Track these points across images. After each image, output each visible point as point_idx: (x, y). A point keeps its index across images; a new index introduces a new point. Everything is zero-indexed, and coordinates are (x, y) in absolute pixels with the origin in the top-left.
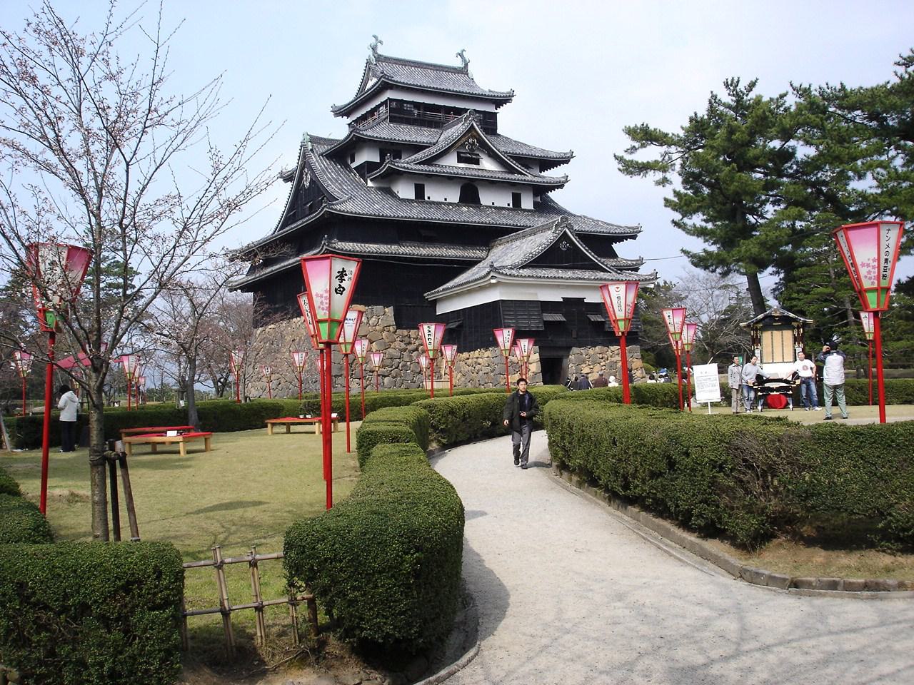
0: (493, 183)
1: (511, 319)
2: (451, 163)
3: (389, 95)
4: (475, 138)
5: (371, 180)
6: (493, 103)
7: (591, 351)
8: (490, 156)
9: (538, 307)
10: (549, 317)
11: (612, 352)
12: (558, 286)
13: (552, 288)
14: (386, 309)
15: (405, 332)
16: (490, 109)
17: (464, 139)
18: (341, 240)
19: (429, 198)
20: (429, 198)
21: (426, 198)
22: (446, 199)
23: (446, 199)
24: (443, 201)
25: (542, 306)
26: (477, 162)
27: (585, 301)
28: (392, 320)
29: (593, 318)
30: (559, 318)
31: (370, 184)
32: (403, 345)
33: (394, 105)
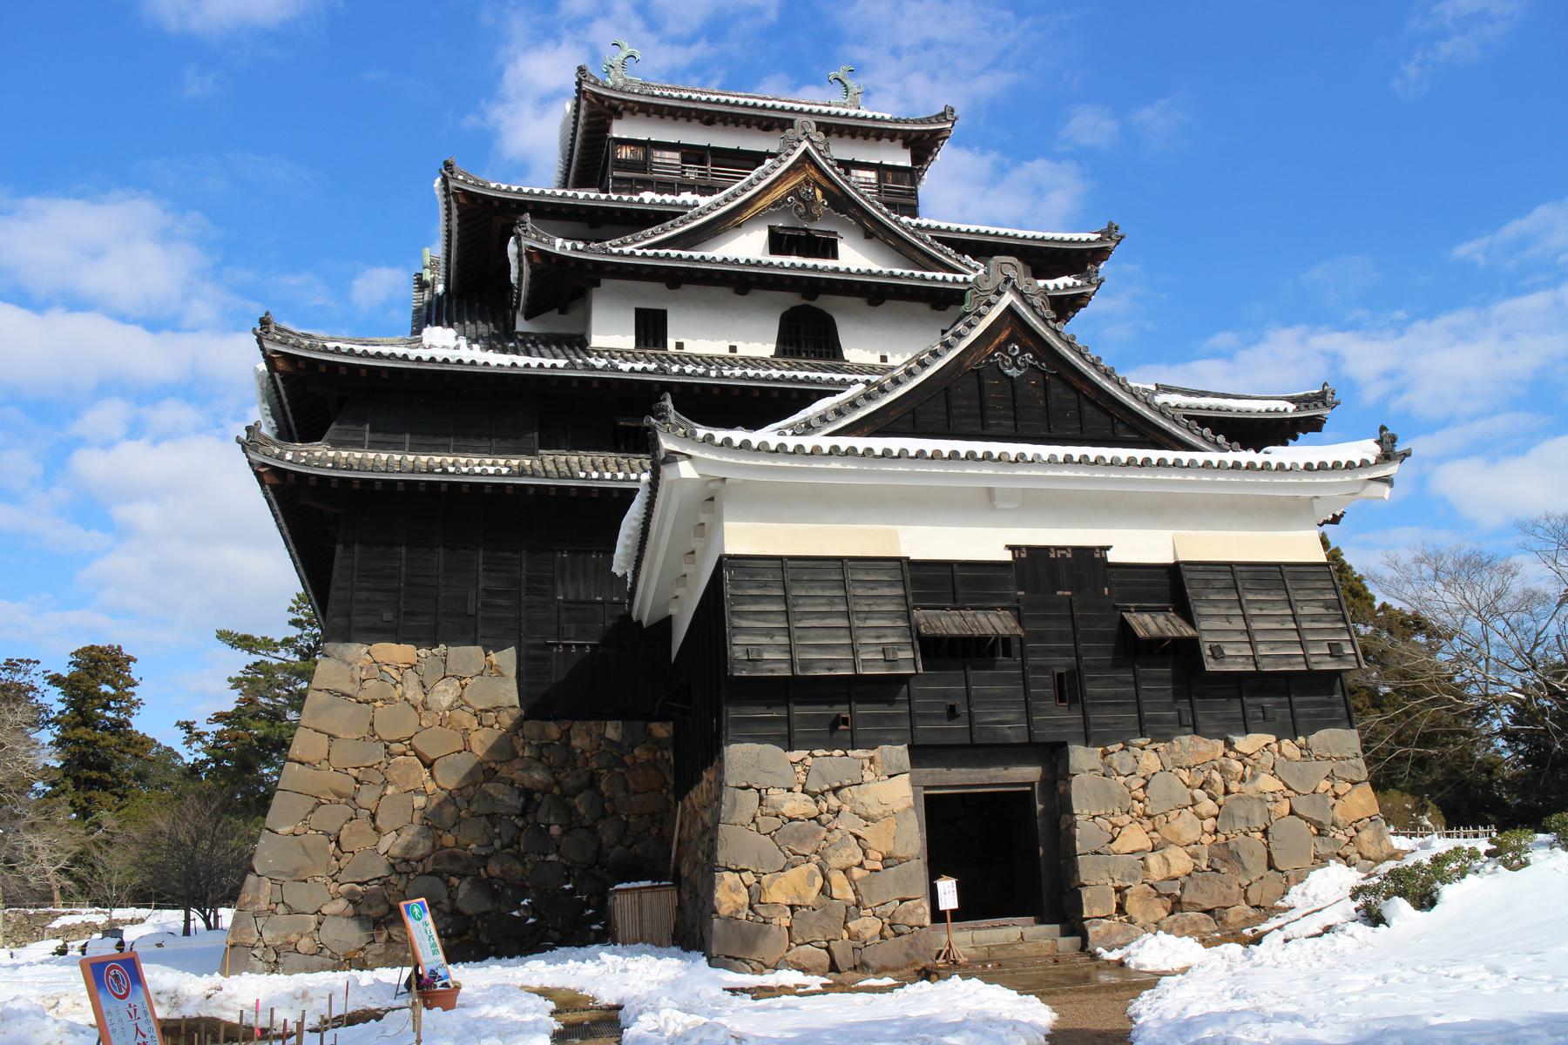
0: (873, 294)
1: (769, 633)
2: (747, 247)
3: (619, 130)
4: (817, 184)
5: (528, 316)
6: (905, 146)
7: (1150, 761)
8: (868, 235)
9: (891, 584)
10: (948, 622)
11: (1242, 758)
12: (987, 504)
13: (975, 511)
14: (494, 657)
15: (553, 730)
16: (903, 159)
17: (781, 190)
18: (336, 445)
19: (680, 346)
20: (680, 346)
21: (671, 347)
22: (733, 349)
23: (733, 349)
24: (726, 352)
25: (916, 582)
26: (835, 256)
27: (1112, 557)
28: (508, 692)
29: (1150, 624)
30: (995, 622)
31: (522, 325)
32: (538, 776)
33: (625, 153)
